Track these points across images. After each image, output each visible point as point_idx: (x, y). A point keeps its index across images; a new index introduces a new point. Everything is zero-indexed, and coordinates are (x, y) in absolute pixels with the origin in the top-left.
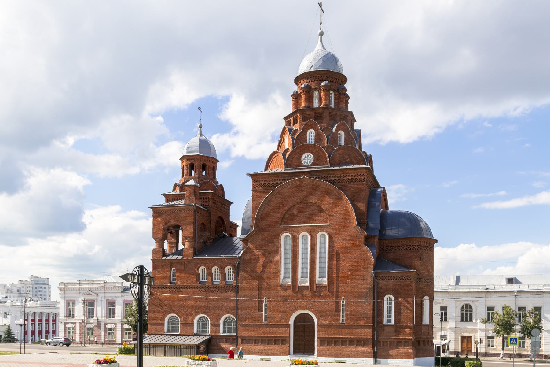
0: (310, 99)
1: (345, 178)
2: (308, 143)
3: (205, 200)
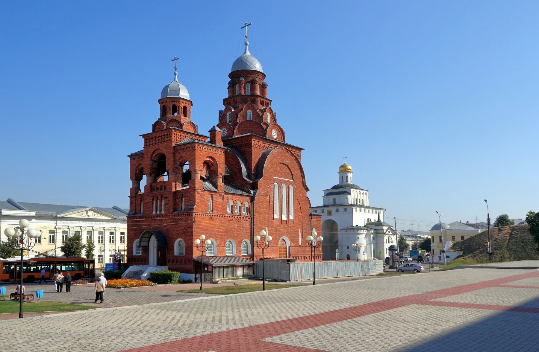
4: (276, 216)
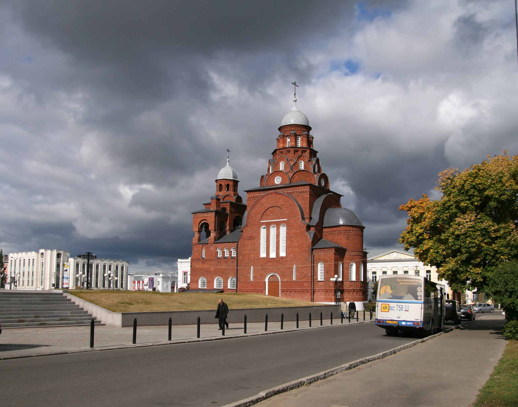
4: (263, 255)
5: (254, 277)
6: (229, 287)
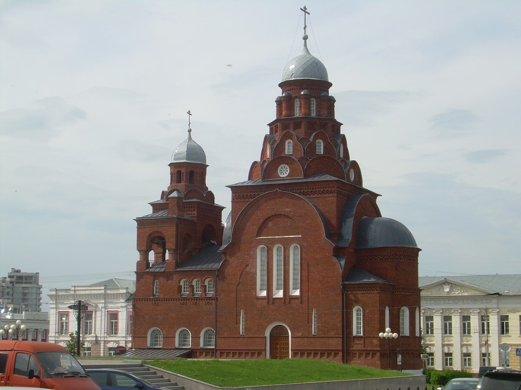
0: (291, 108)
1: (317, 190)
2: (286, 153)
3: (190, 209)
5: (246, 329)
6: (202, 345)
